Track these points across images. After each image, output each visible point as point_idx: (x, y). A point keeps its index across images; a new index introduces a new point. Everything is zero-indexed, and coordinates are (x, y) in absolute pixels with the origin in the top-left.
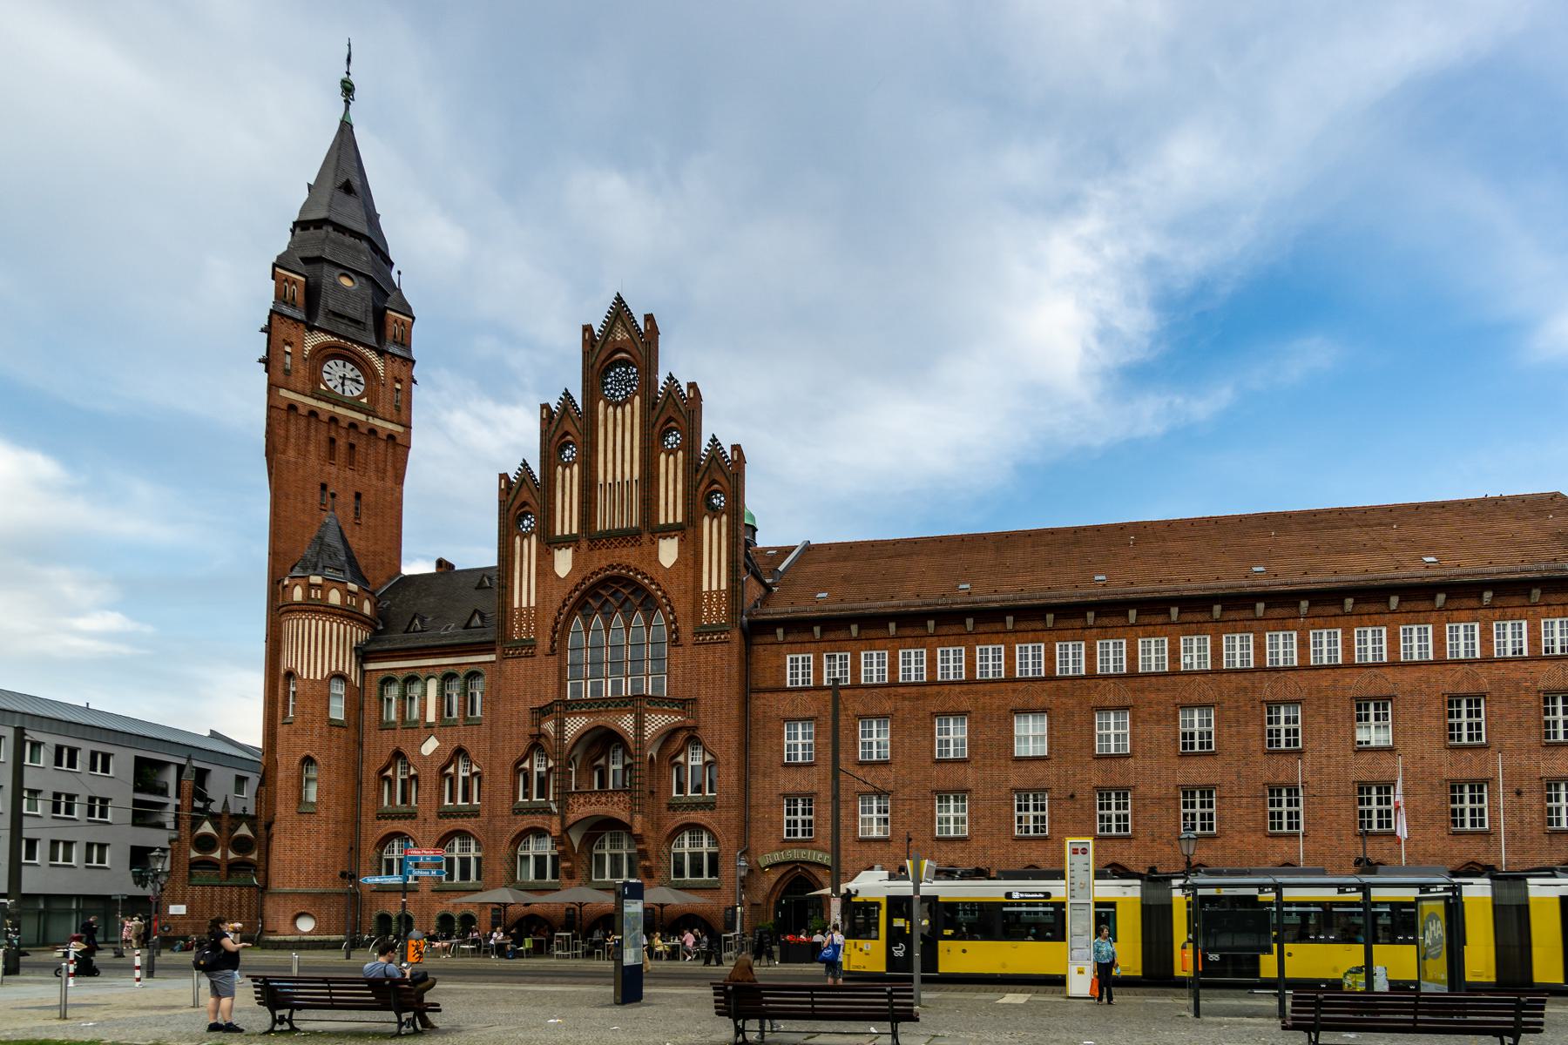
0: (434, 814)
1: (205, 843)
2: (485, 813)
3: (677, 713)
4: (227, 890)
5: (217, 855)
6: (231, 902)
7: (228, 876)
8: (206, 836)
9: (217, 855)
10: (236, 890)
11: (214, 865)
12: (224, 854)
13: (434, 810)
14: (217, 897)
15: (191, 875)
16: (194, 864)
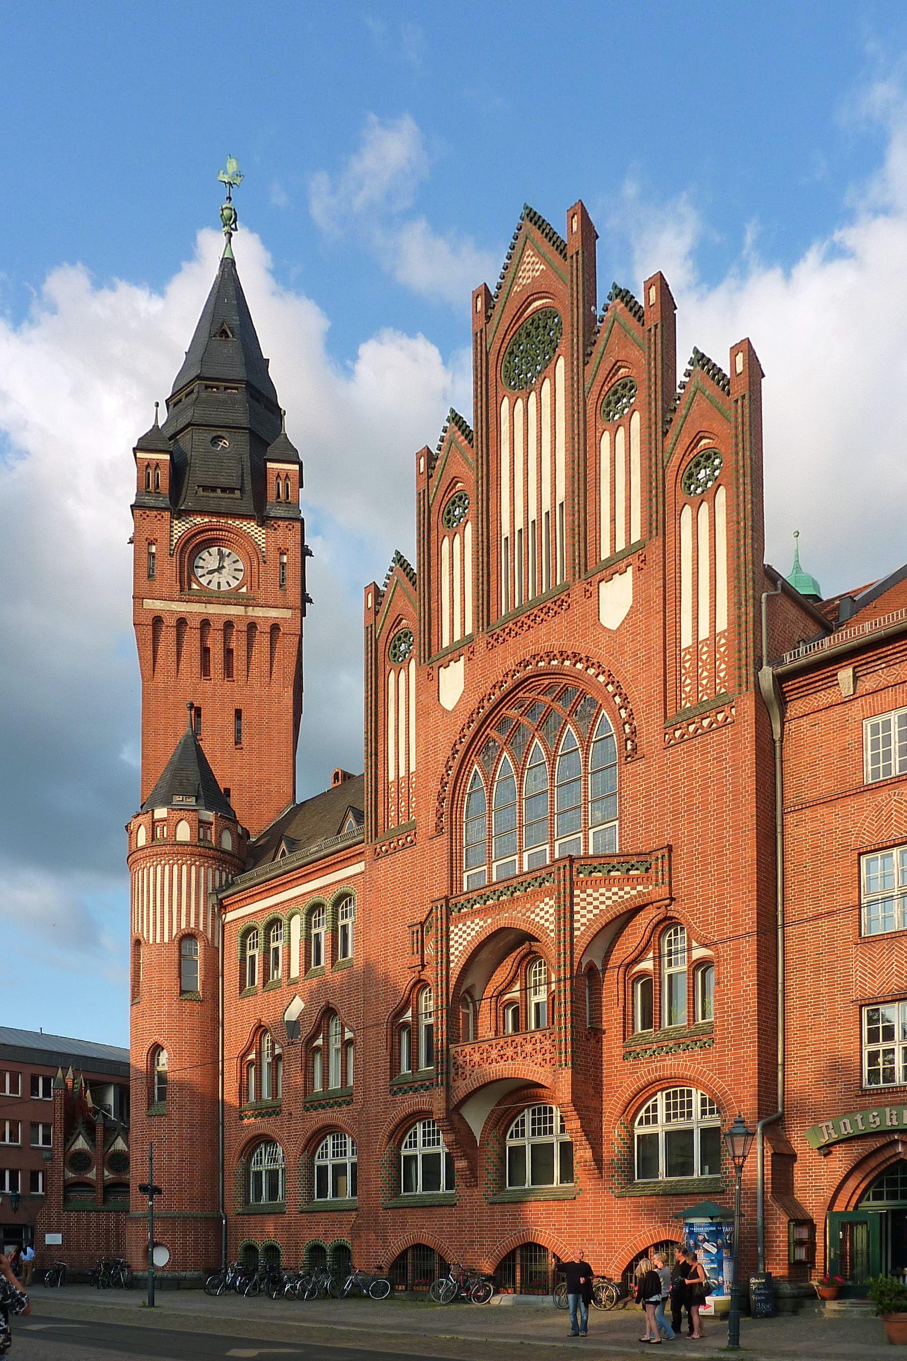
0: (300, 1105)
1: (80, 1161)
2: (359, 1096)
3: (633, 882)
4: (103, 1215)
5: (92, 1175)
6: (108, 1231)
7: (105, 1201)
8: (80, 1153)
9: (92, 1175)
10: (112, 1215)
11: (87, 1185)
12: (100, 1174)
13: (301, 1099)
14: (93, 1225)
15: (66, 1199)
16: (69, 1187)
